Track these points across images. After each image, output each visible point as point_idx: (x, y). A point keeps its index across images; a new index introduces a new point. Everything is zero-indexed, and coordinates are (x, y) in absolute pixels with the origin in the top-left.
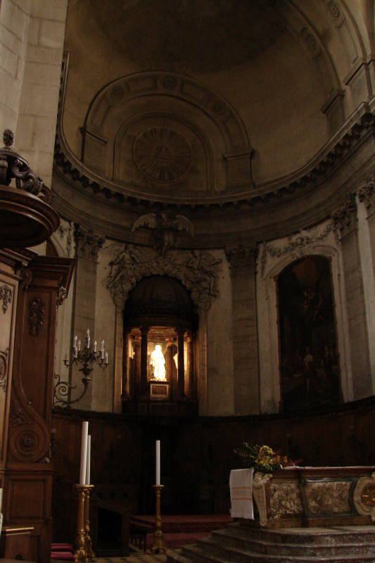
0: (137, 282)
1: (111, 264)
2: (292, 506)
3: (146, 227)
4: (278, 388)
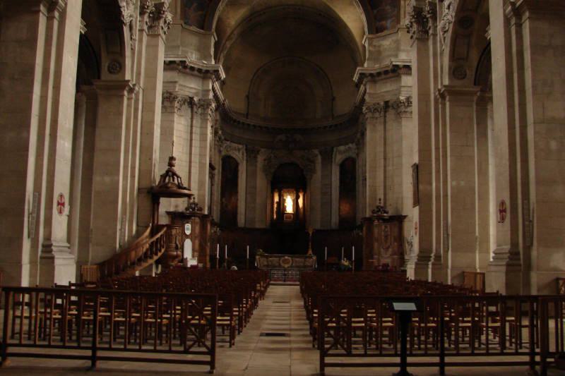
1: (265, 160)
2: (266, 263)
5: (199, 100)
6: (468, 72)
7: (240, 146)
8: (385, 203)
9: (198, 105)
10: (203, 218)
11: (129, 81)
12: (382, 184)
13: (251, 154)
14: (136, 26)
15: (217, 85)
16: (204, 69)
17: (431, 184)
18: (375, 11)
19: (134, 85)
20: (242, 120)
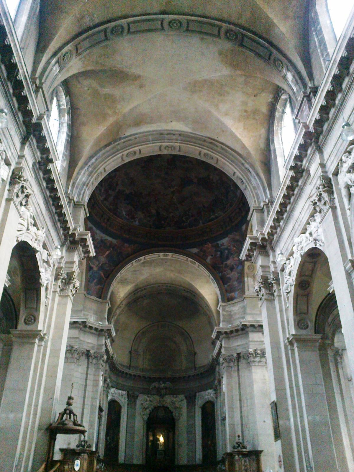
0: (152, 410)
3: (155, 387)
4: (201, 454)
5: (94, 353)
6: (309, 323)
7: (124, 392)
8: (243, 439)
9: (93, 357)
10: (92, 454)
11: (40, 331)
12: (240, 422)
13: (132, 398)
14: (51, 289)
15: (108, 342)
16: (100, 328)
17: (289, 419)
18: (226, 286)
19: (45, 334)
20: (126, 371)
